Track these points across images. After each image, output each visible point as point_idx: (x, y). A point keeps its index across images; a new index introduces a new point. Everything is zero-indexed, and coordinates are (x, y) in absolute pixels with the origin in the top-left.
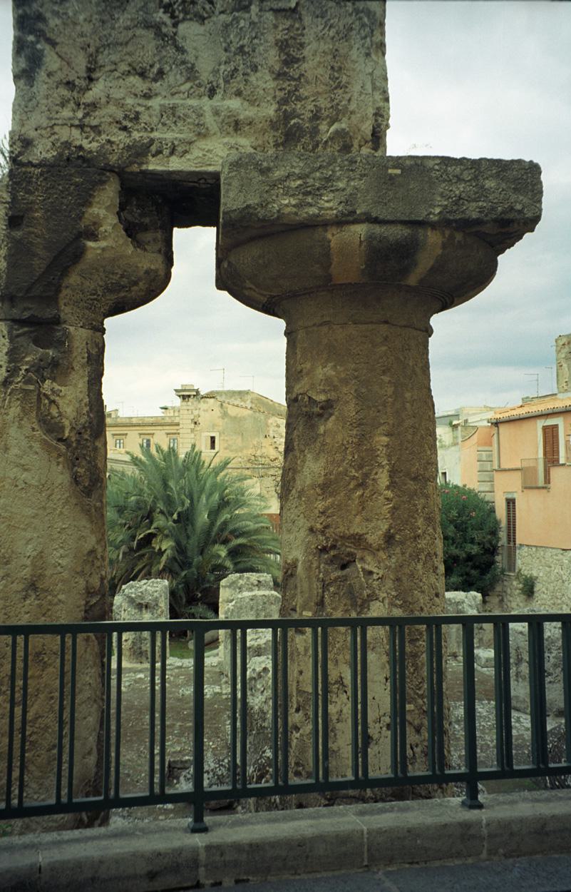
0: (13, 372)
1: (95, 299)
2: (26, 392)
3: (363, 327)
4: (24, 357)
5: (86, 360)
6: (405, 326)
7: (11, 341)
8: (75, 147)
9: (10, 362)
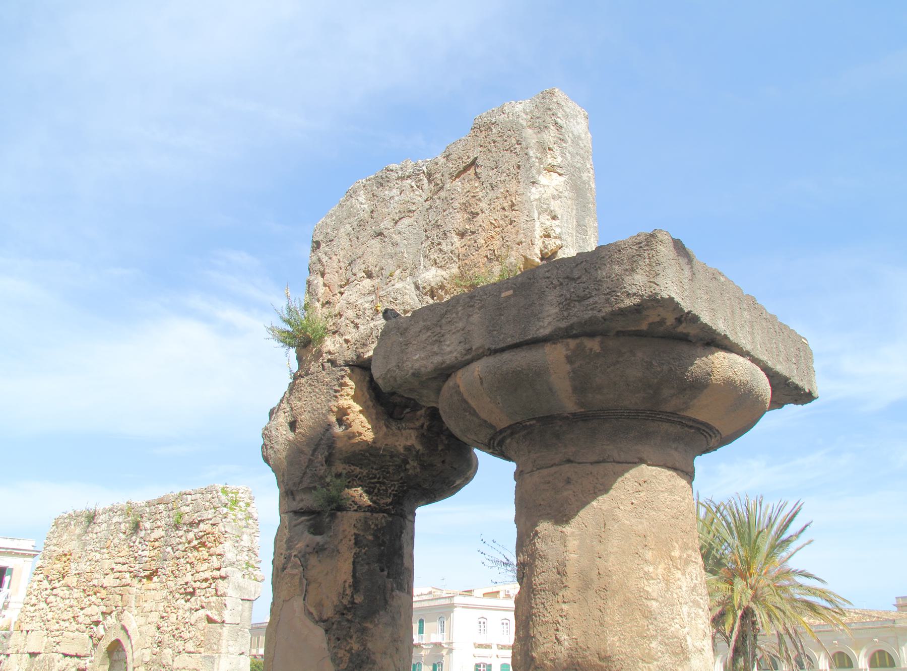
0: (288, 558)
1: (377, 483)
2: (294, 575)
3: (545, 472)
4: (297, 544)
5: (353, 541)
7: (290, 531)
8: (326, 353)
9: (287, 550)
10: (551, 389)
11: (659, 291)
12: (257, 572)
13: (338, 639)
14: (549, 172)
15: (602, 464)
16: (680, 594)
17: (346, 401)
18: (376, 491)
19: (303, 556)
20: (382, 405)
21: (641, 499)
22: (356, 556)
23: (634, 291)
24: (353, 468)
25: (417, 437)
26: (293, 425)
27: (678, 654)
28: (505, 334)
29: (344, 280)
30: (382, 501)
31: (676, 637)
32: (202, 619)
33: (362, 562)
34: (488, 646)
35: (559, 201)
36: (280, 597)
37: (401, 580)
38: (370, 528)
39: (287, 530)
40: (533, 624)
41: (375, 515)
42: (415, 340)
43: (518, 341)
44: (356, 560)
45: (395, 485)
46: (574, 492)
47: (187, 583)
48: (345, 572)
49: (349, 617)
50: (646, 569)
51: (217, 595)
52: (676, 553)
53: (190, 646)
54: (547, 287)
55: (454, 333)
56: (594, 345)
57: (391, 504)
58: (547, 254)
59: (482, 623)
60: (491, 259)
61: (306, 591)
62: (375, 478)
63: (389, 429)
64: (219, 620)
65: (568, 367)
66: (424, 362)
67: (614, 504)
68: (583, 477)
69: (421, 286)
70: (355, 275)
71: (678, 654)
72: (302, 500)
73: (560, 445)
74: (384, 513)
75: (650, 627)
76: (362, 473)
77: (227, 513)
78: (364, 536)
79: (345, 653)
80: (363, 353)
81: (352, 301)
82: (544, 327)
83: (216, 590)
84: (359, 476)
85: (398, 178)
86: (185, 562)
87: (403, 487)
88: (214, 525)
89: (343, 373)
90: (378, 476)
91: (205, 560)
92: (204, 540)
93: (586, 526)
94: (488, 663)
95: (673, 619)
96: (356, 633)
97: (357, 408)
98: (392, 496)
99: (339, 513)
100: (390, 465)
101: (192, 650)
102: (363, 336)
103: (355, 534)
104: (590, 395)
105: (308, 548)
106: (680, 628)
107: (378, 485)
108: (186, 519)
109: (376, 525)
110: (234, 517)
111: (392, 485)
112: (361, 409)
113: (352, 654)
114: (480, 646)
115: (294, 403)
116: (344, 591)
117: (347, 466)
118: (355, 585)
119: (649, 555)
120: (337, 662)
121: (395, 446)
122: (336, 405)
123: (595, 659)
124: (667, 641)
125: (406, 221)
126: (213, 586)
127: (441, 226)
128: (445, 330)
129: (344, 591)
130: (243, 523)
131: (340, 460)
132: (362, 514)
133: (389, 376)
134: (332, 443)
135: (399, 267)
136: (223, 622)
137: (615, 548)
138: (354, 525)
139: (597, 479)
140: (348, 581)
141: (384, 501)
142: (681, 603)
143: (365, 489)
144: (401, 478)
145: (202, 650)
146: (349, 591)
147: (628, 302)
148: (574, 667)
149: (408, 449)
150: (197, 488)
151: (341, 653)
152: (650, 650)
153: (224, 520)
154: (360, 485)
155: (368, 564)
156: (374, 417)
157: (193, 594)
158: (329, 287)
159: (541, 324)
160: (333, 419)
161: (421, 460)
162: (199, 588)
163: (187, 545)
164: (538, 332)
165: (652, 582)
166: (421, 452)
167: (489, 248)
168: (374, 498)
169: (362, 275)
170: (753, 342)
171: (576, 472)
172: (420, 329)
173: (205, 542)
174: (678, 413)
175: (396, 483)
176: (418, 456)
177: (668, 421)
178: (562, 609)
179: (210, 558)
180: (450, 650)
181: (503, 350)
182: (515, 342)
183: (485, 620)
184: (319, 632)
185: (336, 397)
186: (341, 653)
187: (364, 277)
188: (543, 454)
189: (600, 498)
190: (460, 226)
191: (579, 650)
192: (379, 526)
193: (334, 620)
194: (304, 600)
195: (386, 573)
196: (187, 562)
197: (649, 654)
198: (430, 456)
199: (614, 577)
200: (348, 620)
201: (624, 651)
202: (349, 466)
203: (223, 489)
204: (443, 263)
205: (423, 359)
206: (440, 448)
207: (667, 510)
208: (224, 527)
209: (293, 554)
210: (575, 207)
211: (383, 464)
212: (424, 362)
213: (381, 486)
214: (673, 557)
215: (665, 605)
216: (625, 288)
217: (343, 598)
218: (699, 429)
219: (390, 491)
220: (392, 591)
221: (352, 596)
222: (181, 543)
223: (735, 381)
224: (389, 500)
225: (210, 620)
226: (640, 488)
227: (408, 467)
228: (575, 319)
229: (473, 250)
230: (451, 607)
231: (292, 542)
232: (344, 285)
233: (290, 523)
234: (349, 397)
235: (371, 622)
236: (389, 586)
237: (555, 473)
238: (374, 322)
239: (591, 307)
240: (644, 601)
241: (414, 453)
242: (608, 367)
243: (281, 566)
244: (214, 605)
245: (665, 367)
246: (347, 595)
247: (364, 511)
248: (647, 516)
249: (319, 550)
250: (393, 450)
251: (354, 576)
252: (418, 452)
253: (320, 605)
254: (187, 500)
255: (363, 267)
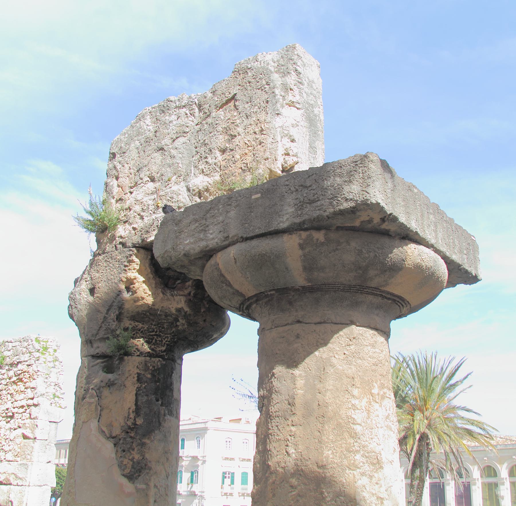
0: (87, 390)
1: (155, 335)
2: (90, 404)
3: (281, 329)
4: (94, 380)
5: (136, 378)
6: (320, 323)
7: (89, 370)
8: (118, 237)
9: (86, 384)
10: (287, 268)
11: (369, 198)
12: (61, 401)
13: (124, 451)
14: (290, 106)
15: (324, 324)
16: (377, 421)
17: (133, 274)
18: (154, 341)
19: (99, 389)
20: (159, 277)
21: (351, 350)
22: (138, 389)
23: (351, 197)
24: (137, 324)
25: (185, 301)
26: (92, 291)
27: (375, 464)
28: (254, 226)
29: (133, 183)
30: (158, 349)
31: (374, 452)
32: (19, 436)
33: (142, 394)
34: (232, 459)
35: (296, 129)
36: (80, 420)
37: (172, 408)
38: (149, 369)
39: (87, 370)
40: (270, 441)
41: (152, 359)
42: (186, 229)
43: (264, 232)
44: (138, 393)
45: (168, 337)
46: (302, 345)
47: (7, 409)
48: (130, 402)
49: (132, 435)
50: (353, 402)
51: (31, 418)
52: (375, 391)
53: (9, 457)
54: (286, 192)
55: (215, 225)
56: (319, 236)
57: (165, 351)
58: (286, 167)
59: (228, 442)
60: (245, 170)
61: (100, 415)
62: (153, 332)
63: (164, 295)
64: (32, 437)
65: (300, 252)
66: (193, 246)
67: (331, 354)
68: (308, 333)
69: (191, 189)
70: (142, 179)
71: (375, 464)
72: (98, 347)
73: (292, 310)
74: (159, 357)
75: (355, 444)
76: (144, 328)
77: (39, 357)
78: (144, 374)
79: (129, 461)
80: (147, 238)
81: (139, 199)
82: (283, 222)
83: (30, 415)
84: (142, 330)
85: (176, 107)
86: (6, 393)
87: (174, 339)
88: (29, 365)
89: (131, 253)
90: (155, 330)
91: (22, 392)
92: (21, 377)
93: (310, 370)
94: (232, 472)
95: (372, 439)
96: (137, 446)
97: (142, 279)
98: (166, 345)
99: (126, 358)
100: (164, 323)
101: (11, 459)
102: (147, 225)
103: (137, 373)
104: (316, 273)
105: (102, 383)
106: (377, 445)
107: (155, 337)
108: (8, 361)
109: (154, 367)
110: (44, 360)
111: (166, 337)
112: (144, 279)
113: (134, 462)
114: (226, 459)
115: (94, 275)
116: (129, 415)
117: (132, 323)
118: (137, 411)
119: (356, 392)
120: (122, 468)
121: (170, 308)
122: (126, 277)
123: (314, 467)
124: (367, 455)
125: (181, 140)
126: (28, 411)
127: (208, 144)
128: (209, 222)
129: (129, 415)
130: (52, 364)
131: (127, 318)
132: (143, 358)
133: (166, 255)
134: (122, 305)
135: (175, 174)
136: (35, 438)
137: (331, 386)
138: (137, 366)
139: (319, 335)
140: (132, 408)
141: (160, 349)
142: (378, 427)
143: (146, 339)
144: (173, 332)
145: (18, 459)
146: (132, 416)
147: (346, 205)
148: (299, 473)
149: (179, 310)
150: (17, 338)
151: (126, 461)
152: (355, 461)
153: (37, 362)
154: (142, 337)
155: (147, 395)
156: (154, 286)
157: (12, 417)
158: (122, 188)
159: (281, 219)
160: (123, 287)
161: (188, 319)
162: (17, 413)
163: (8, 380)
164: (278, 226)
165: (357, 411)
166: (188, 313)
167: (243, 162)
168: (153, 347)
169: (147, 180)
170: (436, 238)
171: (304, 330)
172: (190, 221)
173: (22, 379)
174: (380, 288)
175: (169, 336)
176: (186, 316)
177: (373, 294)
178: (291, 430)
179: (26, 390)
180: (204, 462)
181: (252, 238)
182: (261, 232)
183: (230, 440)
184: (109, 445)
185: (126, 270)
186: (126, 461)
187: (148, 181)
188: (279, 316)
189: (321, 349)
190: (222, 144)
191: (303, 460)
192: (156, 368)
193: (120, 437)
194: (99, 422)
195: (160, 402)
196: (8, 393)
197: (353, 464)
198: (195, 316)
199: (330, 408)
200: (131, 437)
201: (336, 461)
202: (134, 322)
203: (36, 339)
204: (209, 172)
205: (192, 243)
206: (202, 311)
207: (369, 359)
208: (37, 367)
209: (91, 387)
210: (308, 134)
211: (160, 321)
212: (193, 246)
213: (158, 338)
214: (373, 393)
215: (366, 429)
216: (344, 194)
217: (128, 420)
218: (394, 300)
219: (164, 341)
220: (165, 415)
221: (135, 419)
222: (3, 379)
223: (422, 266)
224: (164, 348)
225: (25, 437)
226: (351, 343)
227: (178, 323)
228: (306, 217)
229: (231, 163)
230: (205, 429)
231: (90, 378)
232: (133, 186)
233: (88, 364)
234: (135, 271)
235: (148, 438)
236: (162, 412)
237: (288, 330)
238: (155, 215)
239: (319, 208)
240: (351, 425)
241: (183, 313)
242: (330, 253)
243: (81, 396)
244: (29, 426)
245: (371, 254)
246: (131, 418)
247: (145, 356)
248: (355, 364)
249: (110, 384)
250: (167, 311)
251: (136, 404)
252: (186, 313)
253: (110, 426)
254: (9, 347)
255: (148, 173)
